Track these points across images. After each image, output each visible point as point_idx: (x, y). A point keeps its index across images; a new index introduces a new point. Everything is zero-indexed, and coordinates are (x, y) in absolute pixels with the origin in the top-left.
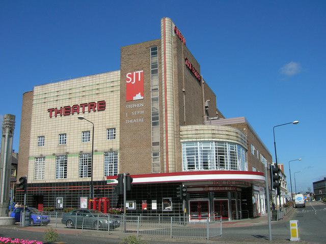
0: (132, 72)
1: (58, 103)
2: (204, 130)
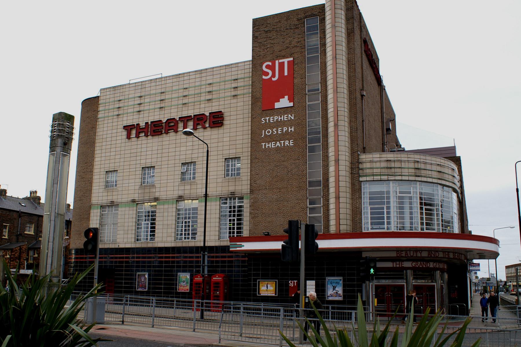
1: (141, 116)
2: (401, 161)
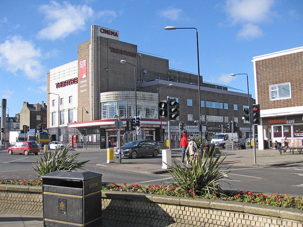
0: (82, 61)
